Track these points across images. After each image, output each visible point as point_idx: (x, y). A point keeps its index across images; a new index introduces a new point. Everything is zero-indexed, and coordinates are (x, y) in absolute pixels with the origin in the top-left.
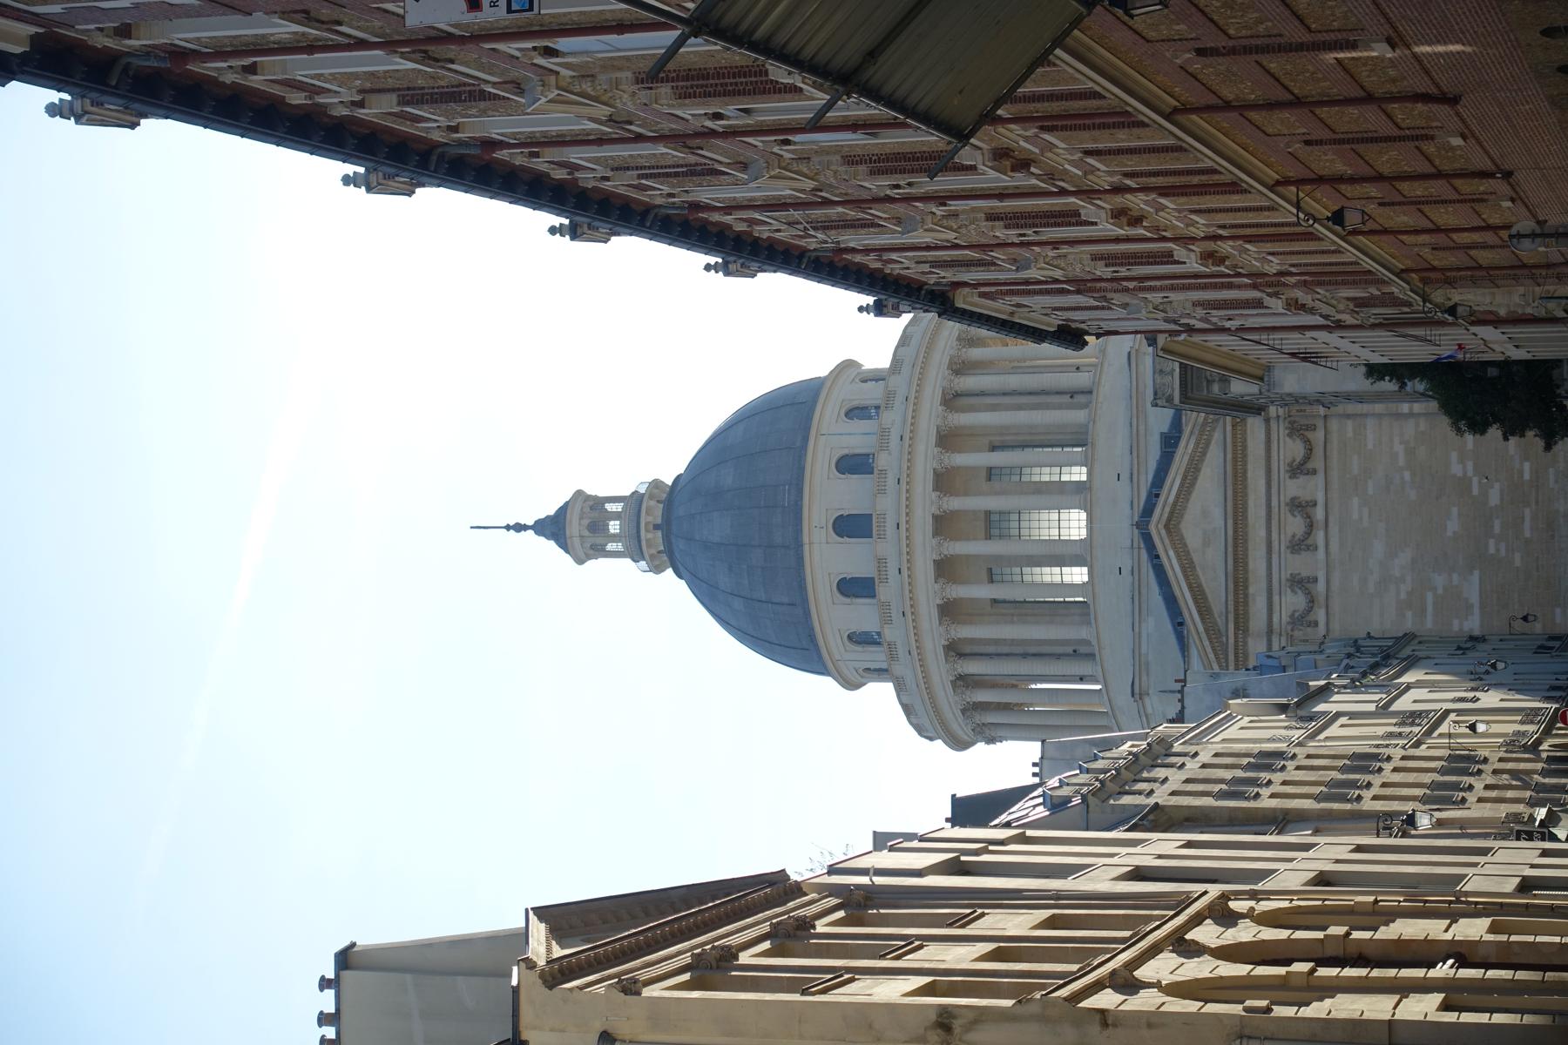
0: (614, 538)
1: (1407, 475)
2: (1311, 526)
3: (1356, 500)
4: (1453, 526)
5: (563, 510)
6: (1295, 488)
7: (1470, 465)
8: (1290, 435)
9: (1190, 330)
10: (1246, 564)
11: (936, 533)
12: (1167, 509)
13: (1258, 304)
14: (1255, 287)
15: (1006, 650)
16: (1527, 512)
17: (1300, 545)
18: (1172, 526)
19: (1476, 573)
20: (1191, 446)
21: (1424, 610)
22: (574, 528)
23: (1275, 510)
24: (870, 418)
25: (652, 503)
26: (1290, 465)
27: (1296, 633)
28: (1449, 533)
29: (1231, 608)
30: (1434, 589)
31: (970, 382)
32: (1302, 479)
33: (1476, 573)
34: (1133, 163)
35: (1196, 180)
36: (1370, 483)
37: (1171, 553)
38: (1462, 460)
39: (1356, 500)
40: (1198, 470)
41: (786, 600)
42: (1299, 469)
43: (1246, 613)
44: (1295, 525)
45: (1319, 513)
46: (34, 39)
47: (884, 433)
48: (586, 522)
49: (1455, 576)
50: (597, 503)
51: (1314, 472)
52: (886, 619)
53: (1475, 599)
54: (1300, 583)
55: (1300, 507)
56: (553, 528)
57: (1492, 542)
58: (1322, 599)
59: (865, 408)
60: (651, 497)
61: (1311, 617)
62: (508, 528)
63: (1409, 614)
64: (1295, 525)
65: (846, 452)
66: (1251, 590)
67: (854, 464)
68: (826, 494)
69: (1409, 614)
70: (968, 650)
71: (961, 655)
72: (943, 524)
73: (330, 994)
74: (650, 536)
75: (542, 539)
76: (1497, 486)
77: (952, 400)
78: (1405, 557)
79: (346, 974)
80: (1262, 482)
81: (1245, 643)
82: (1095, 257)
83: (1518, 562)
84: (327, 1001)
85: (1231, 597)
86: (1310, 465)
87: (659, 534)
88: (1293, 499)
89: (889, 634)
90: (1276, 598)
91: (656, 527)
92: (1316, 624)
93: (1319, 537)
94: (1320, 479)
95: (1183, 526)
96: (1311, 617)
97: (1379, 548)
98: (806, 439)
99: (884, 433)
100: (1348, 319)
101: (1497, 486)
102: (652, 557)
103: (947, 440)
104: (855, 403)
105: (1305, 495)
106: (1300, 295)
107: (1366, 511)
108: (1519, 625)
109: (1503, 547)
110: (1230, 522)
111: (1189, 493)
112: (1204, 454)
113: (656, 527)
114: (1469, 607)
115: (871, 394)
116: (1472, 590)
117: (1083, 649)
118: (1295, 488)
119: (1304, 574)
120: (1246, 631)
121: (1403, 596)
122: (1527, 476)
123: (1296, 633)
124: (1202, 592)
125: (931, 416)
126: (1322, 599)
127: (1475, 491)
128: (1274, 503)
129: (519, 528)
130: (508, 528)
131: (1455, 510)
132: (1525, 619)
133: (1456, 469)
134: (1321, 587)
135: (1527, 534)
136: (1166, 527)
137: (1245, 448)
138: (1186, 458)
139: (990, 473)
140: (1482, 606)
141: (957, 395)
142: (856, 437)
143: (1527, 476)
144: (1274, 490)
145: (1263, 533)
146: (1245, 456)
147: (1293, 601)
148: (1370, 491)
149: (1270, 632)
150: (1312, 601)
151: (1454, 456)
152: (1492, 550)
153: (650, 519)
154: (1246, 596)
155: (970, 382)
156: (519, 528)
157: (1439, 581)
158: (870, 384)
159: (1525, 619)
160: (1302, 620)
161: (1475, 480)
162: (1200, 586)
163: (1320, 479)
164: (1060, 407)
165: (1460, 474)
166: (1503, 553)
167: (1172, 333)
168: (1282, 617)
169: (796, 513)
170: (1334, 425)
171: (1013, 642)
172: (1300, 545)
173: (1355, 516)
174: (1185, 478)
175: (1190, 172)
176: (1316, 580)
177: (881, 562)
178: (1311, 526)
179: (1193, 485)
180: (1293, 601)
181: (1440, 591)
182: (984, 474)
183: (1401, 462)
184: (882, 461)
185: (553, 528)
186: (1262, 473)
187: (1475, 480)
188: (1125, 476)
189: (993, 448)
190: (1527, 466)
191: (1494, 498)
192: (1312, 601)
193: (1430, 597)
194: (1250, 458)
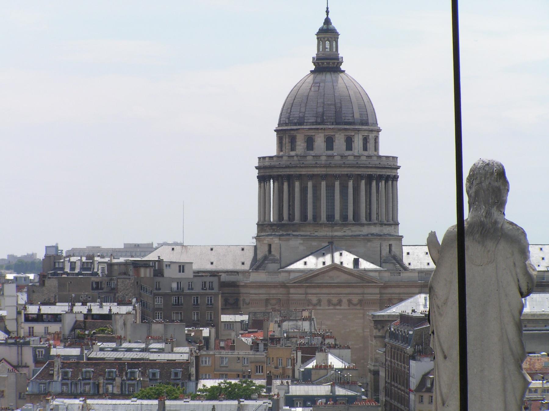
1: (348, 330)
6: (345, 301)
42: (350, 302)
44: (335, 300)
45: (338, 307)
62: (327, 8)
94: (348, 308)
102: (318, 63)
118: (345, 301)
119: (322, 303)
129: (327, 12)
130: (327, 8)
150: (315, 305)
156: (327, 12)
163: (347, 307)
168: (310, 297)
170: (361, 311)
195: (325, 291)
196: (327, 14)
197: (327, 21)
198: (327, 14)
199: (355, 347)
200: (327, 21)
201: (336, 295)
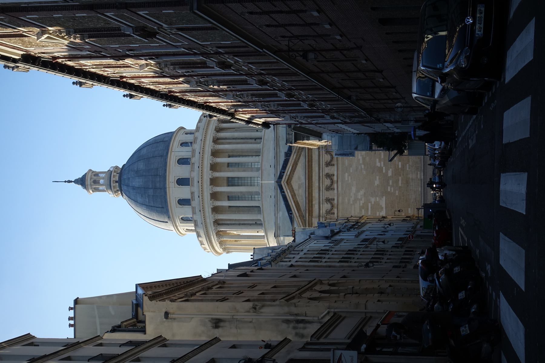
0: (102, 185)
1: (363, 166)
2: (332, 182)
3: (347, 174)
4: (377, 182)
5: (84, 176)
6: (327, 170)
7: (382, 163)
8: (326, 153)
9: (301, 123)
10: (312, 194)
11: (211, 185)
12: (287, 177)
13: (323, 117)
14: (323, 112)
15: (234, 222)
16: (400, 178)
17: (329, 188)
18: (289, 182)
19: (384, 197)
20: (295, 157)
21: (368, 209)
22: (88, 181)
23: (321, 177)
24: (189, 146)
25: (115, 174)
26: (326, 163)
27: (328, 216)
28: (376, 185)
29: (307, 209)
30: (371, 202)
31: (222, 135)
32: (330, 167)
33: (384, 197)
34: (294, 84)
35: (311, 87)
36: (351, 169)
37: (288, 191)
38: (380, 162)
39: (347, 174)
40: (297, 164)
41: (160, 206)
43: (312, 210)
44: (327, 182)
45: (335, 178)
46: (22, 55)
47: (193, 151)
48: (92, 180)
49: (378, 198)
50: (96, 174)
51: (334, 165)
52: (194, 213)
53: (384, 206)
54: (329, 200)
55: (329, 176)
56: (82, 181)
57: (389, 187)
58: (336, 206)
59: (187, 143)
60: (115, 172)
61: (332, 211)
62: (65, 182)
63: (363, 210)
64: (327, 182)
65: (181, 157)
66: (314, 203)
67: (183, 161)
68: (175, 171)
69: (363, 210)
70: (221, 222)
71: (219, 224)
72: (214, 182)
73: (72, 311)
74: (114, 185)
75: (77, 185)
76: (391, 169)
77: (216, 141)
78: (362, 192)
79: (77, 306)
80: (317, 168)
81: (312, 220)
82: (278, 105)
83: (397, 194)
84: (71, 314)
85: (307, 205)
86: (332, 163)
87: (117, 184)
88: (327, 174)
89: (195, 217)
90: (321, 205)
91: (116, 182)
92: (334, 213)
93: (335, 186)
94: (336, 166)
95: (292, 182)
96: (332, 211)
97: (354, 189)
98: (167, 153)
99: (193, 151)
100: (348, 121)
101: (391, 169)
103: (215, 153)
104: (184, 141)
105: (331, 173)
106: (335, 115)
107: (350, 177)
108: (397, 213)
109: (392, 189)
110: (307, 181)
111: (294, 172)
112: (299, 159)
113: (116, 182)
114: (382, 208)
115: (190, 138)
116: (383, 203)
117: (258, 222)
118: (327, 170)
119: (330, 198)
120: (312, 216)
121: (361, 205)
122: (400, 167)
123: (328, 216)
124: (298, 203)
125: (209, 146)
126: (336, 206)
127: (384, 171)
128: (321, 175)
129: (69, 182)
130: (65, 182)
131: (378, 177)
132: (399, 211)
133: (378, 164)
134: (336, 202)
135: (400, 185)
136: (287, 183)
137: (312, 157)
138: (293, 161)
139: (229, 165)
140: (386, 208)
141: (218, 139)
142: (185, 152)
143: (400, 167)
144: (321, 171)
145: (317, 185)
146: (312, 160)
147: (327, 206)
148: (351, 171)
149: (319, 216)
150: (333, 206)
151: (377, 160)
152: (389, 190)
153: (114, 179)
154: (312, 205)
155: (222, 135)
156: (69, 182)
157: (373, 200)
158: (188, 135)
159: (399, 211)
160: (329, 212)
161: (384, 168)
162: (297, 201)
164: (251, 143)
165: (379, 166)
166: (392, 191)
167: (296, 124)
168: (323, 211)
169: (164, 178)
171: (236, 220)
172: (329, 188)
173: (347, 179)
174: (293, 167)
175: (309, 86)
176: (334, 199)
177: (192, 193)
178: (332, 182)
179: (295, 169)
180: (327, 206)
181: (373, 203)
182: (226, 165)
183: (361, 162)
184: (193, 160)
185: (82, 181)
186: (317, 165)
187: (384, 168)
188: (273, 166)
189: (229, 157)
190: (400, 163)
191: (390, 173)
192: (333, 206)
193: (370, 204)
194: (313, 161)
195: (315, 194)
196: (71, 182)
197: (77, 182)
198: (71, 182)
199: (382, 157)
200: (77, 182)
201: (321, 181)
